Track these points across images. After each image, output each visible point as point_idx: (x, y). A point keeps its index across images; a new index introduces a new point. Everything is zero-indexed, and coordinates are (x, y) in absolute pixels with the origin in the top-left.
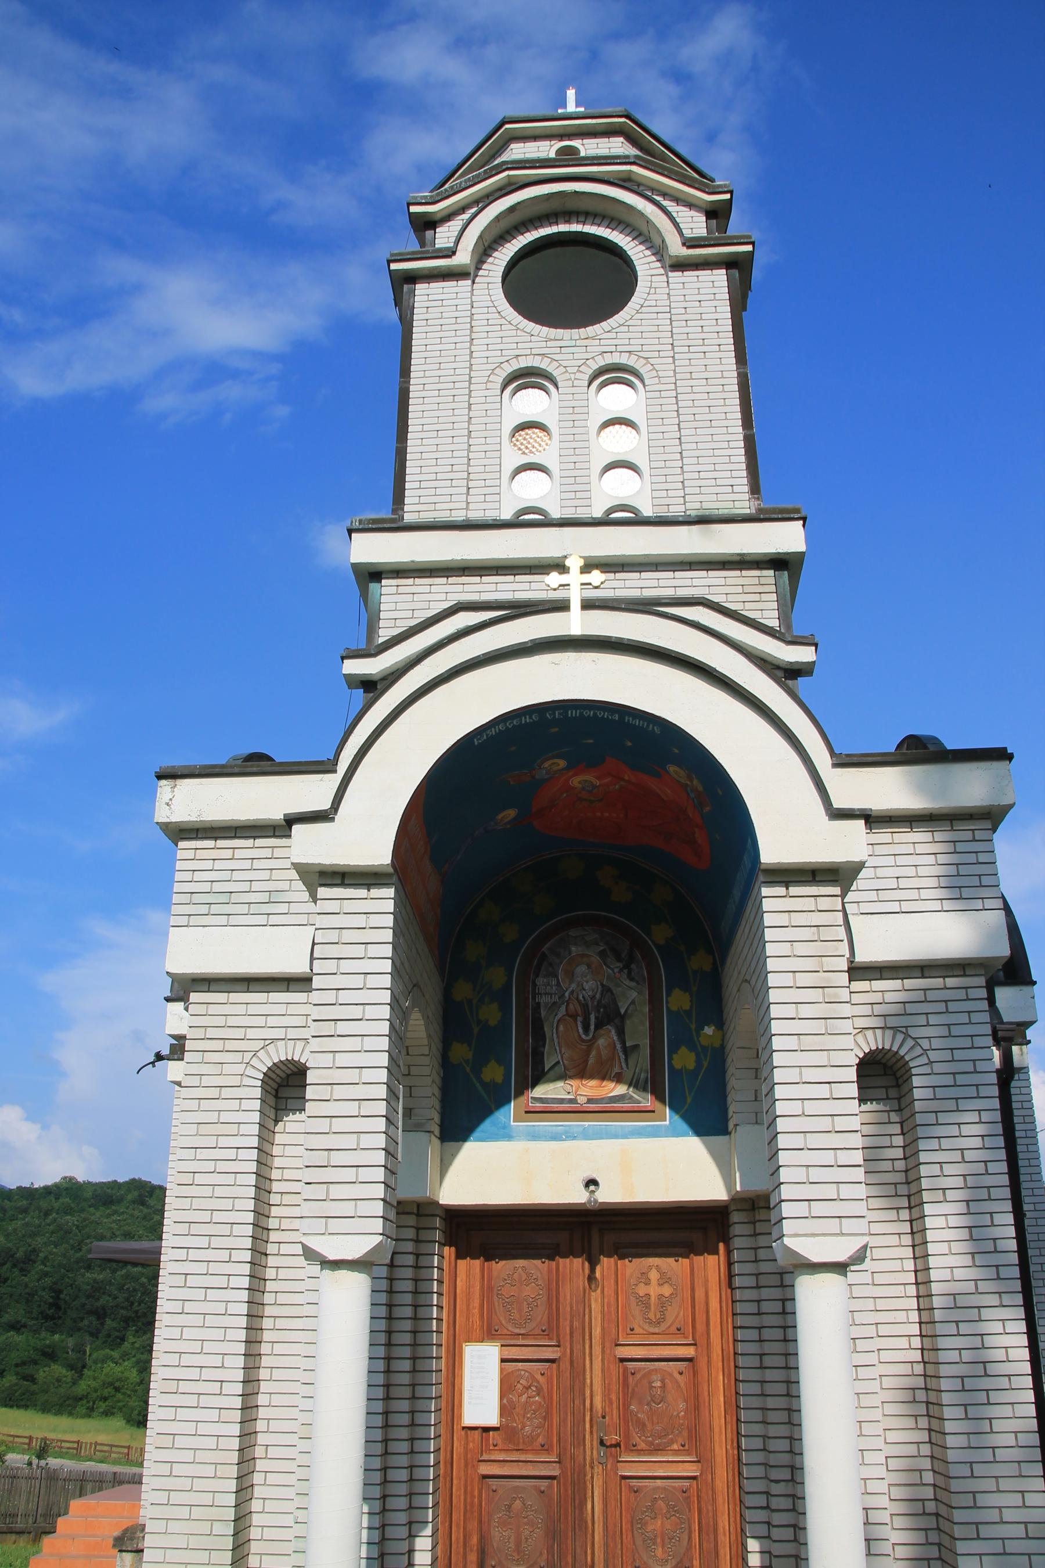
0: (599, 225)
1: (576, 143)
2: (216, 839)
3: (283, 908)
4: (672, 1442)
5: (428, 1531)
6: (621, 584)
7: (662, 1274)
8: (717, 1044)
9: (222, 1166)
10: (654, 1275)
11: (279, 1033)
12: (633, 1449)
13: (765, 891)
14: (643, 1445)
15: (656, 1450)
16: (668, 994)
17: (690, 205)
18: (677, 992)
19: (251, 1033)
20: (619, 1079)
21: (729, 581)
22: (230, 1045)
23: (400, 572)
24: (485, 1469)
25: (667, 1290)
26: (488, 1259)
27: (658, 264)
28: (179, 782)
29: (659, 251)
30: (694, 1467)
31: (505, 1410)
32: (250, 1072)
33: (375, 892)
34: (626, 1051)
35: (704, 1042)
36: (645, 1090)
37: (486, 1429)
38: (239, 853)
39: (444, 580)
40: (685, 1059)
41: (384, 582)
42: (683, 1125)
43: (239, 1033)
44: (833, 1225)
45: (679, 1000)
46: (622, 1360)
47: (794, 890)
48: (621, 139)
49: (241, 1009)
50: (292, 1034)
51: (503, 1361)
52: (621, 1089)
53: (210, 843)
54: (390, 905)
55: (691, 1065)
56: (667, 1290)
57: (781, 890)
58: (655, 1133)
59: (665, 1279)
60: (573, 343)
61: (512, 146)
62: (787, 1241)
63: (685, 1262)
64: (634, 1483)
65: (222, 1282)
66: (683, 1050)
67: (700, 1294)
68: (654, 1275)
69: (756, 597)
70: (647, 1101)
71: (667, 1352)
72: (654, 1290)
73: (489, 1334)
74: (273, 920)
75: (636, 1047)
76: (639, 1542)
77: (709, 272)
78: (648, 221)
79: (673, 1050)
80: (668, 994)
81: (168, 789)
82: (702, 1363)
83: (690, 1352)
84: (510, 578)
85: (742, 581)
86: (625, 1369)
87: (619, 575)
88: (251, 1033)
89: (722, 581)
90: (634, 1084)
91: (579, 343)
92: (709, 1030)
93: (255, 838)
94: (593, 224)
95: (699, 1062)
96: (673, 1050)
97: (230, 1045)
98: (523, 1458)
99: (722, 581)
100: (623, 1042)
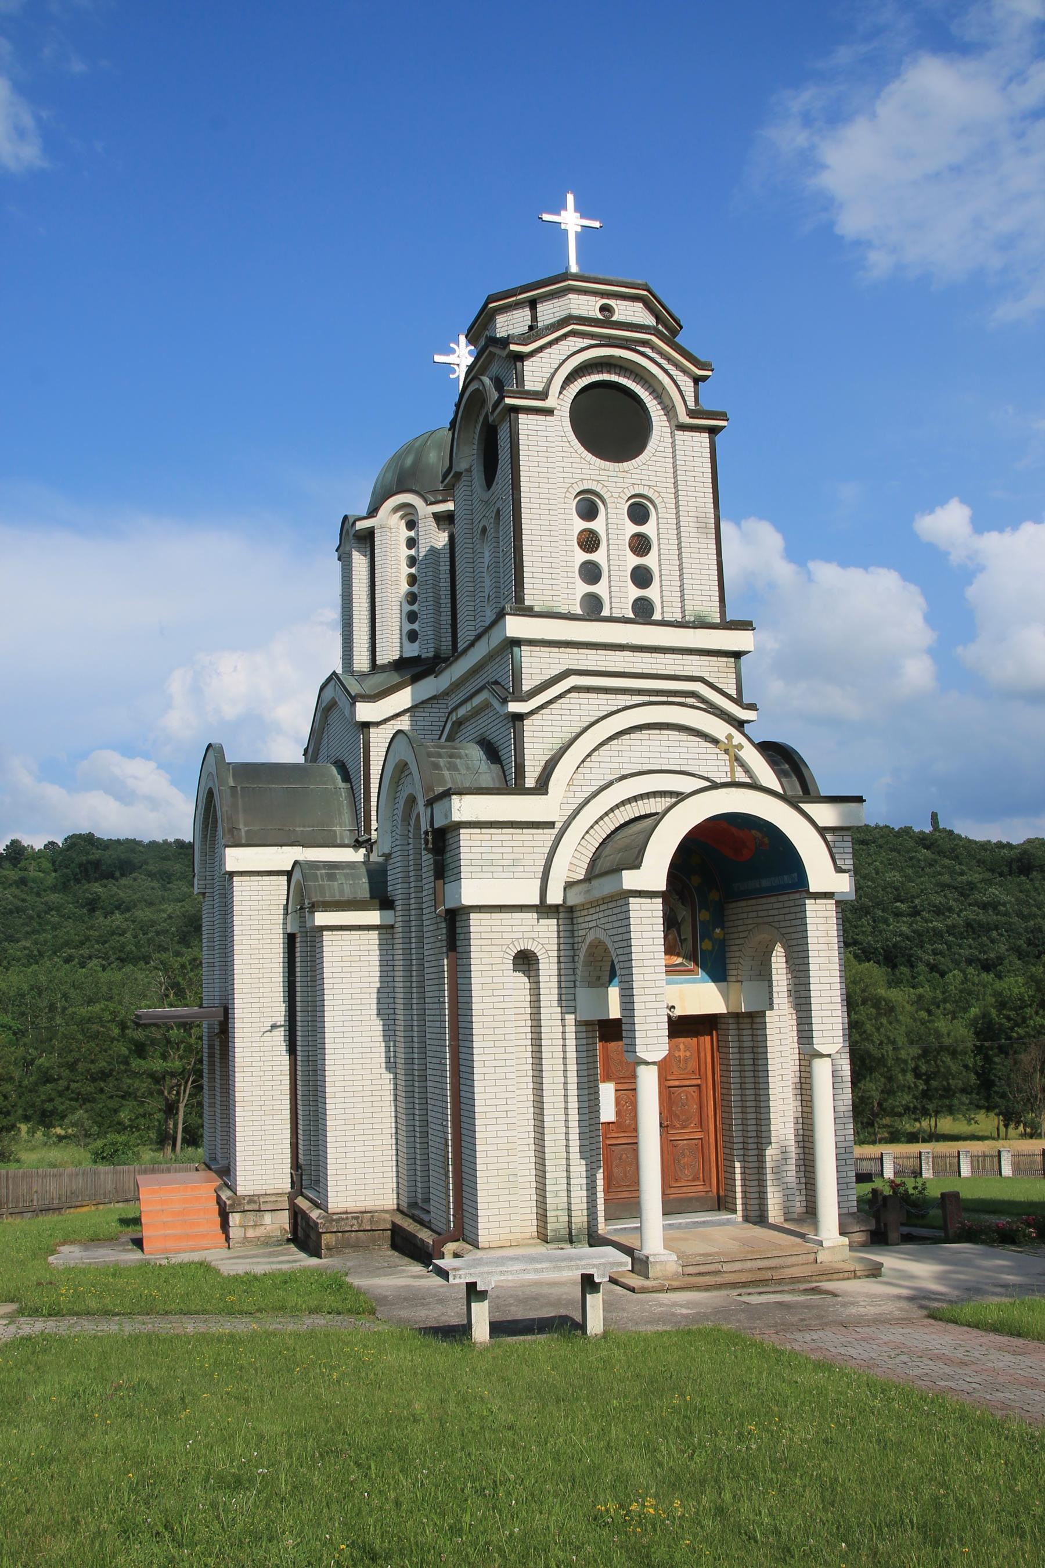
0: (628, 379)
1: (612, 302)
2: (481, 828)
3: (521, 869)
4: (691, 1123)
5: (601, 1170)
6: (653, 661)
7: (686, 1046)
8: (722, 937)
9: (496, 1005)
10: (682, 1046)
11: (520, 935)
12: (674, 1127)
13: (807, 901)
14: (678, 1126)
15: (684, 1127)
16: (700, 912)
17: (685, 371)
18: (703, 911)
19: (505, 935)
20: (678, 955)
21: (712, 664)
22: (494, 942)
23: (531, 642)
24: (609, 1142)
25: (688, 1054)
26: (606, 1042)
27: (665, 418)
28: (463, 797)
29: (669, 410)
30: (700, 1133)
31: (618, 1113)
32: (506, 956)
33: (654, 900)
34: (682, 941)
35: (716, 936)
36: (690, 960)
37: (609, 1123)
38: (494, 837)
39: (557, 650)
40: (707, 945)
41: (523, 648)
42: (707, 977)
43: (499, 935)
44: (830, 1040)
45: (704, 915)
46: (669, 1087)
47: (818, 901)
48: (641, 305)
49: (499, 922)
50: (526, 935)
51: (616, 1090)
52: (679, 960)
53: (478, 831)
54: (661, 907)
55: (710, 947)
56: (688, 1054)
57: (813, 901)
58: (694, 982)
59: (687, 1048)
60: (615, 474)
61: (570, 296)
62: (815, 1046)
63: (695, 1039)
64: (674, 1142)
65: (502, 1063)
66: (706, 940)
67: (702, 1054)
68: (682, 1046)
69: (725, 675)
70: (691, 966)
71: (688, 1083)
72: (682, 1054)
73: (607, 1078)
74: (517, 875)
75: (685, 939)
76: (677, 1168)
77: (698, 434)
78: (664, 388)
79: (702, 940)
80: (700, 912)
81: (458, 801)
82: (704, 1087)
83: (698, 1082)
84: (594, 652)
85: (718, 664)
86: (670, 1092)
87: (654, 655)
88: (505, 935)
89: (707, 663)
90: (685, 957)
91: (619, 474)
92: (718, 931)
93: (502, 828)
94: (624, 377)
95: (713, 946)
96: (702, 940)
97: (494, 942)
98: (626, 1135)
99: (707, 663)
100: (680, 936)
